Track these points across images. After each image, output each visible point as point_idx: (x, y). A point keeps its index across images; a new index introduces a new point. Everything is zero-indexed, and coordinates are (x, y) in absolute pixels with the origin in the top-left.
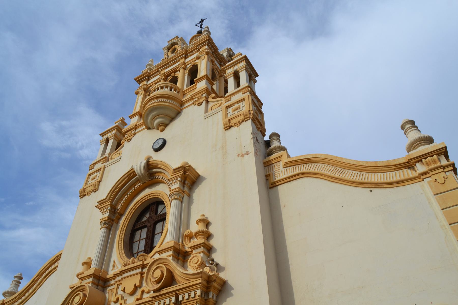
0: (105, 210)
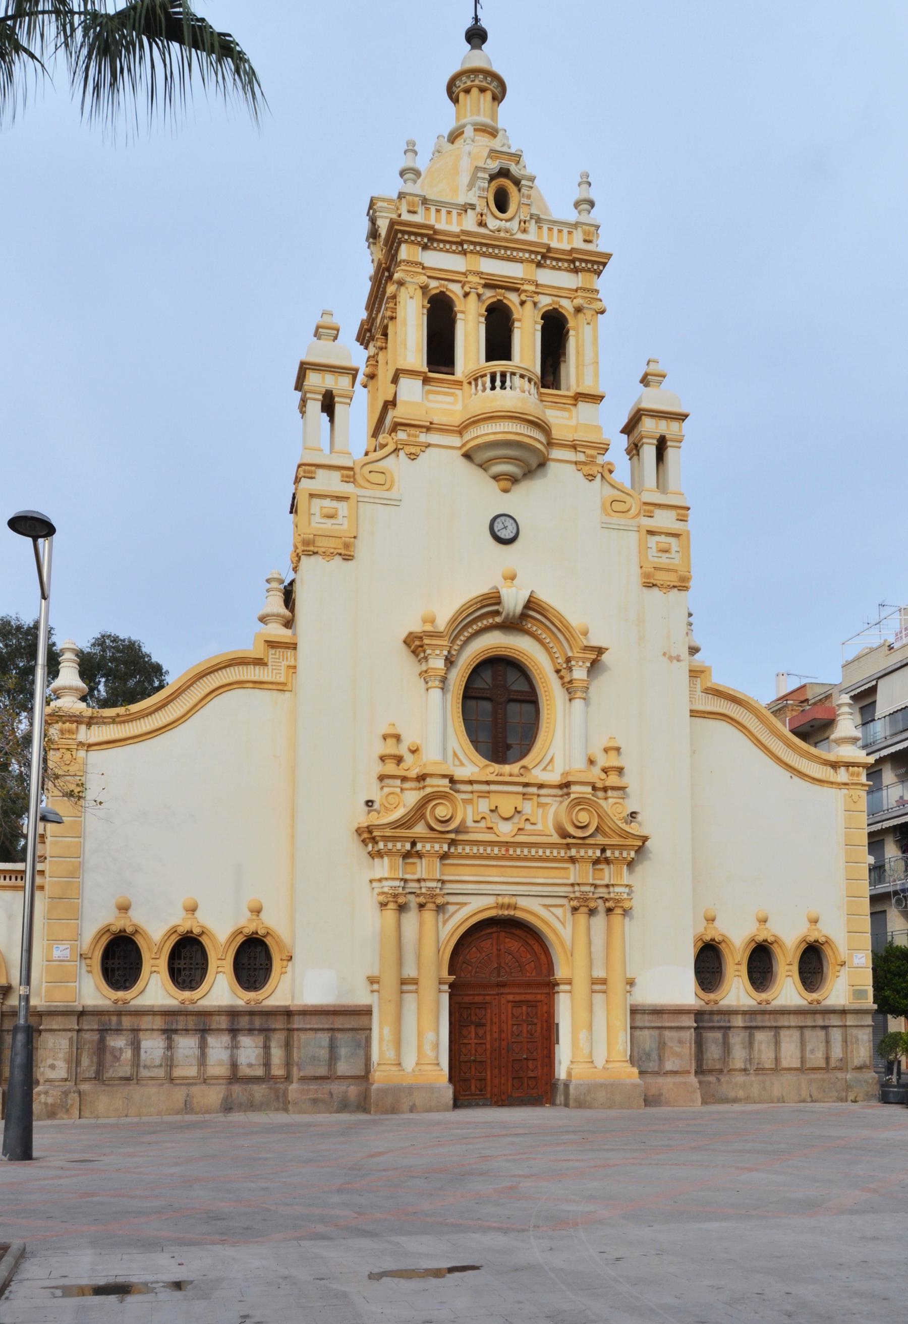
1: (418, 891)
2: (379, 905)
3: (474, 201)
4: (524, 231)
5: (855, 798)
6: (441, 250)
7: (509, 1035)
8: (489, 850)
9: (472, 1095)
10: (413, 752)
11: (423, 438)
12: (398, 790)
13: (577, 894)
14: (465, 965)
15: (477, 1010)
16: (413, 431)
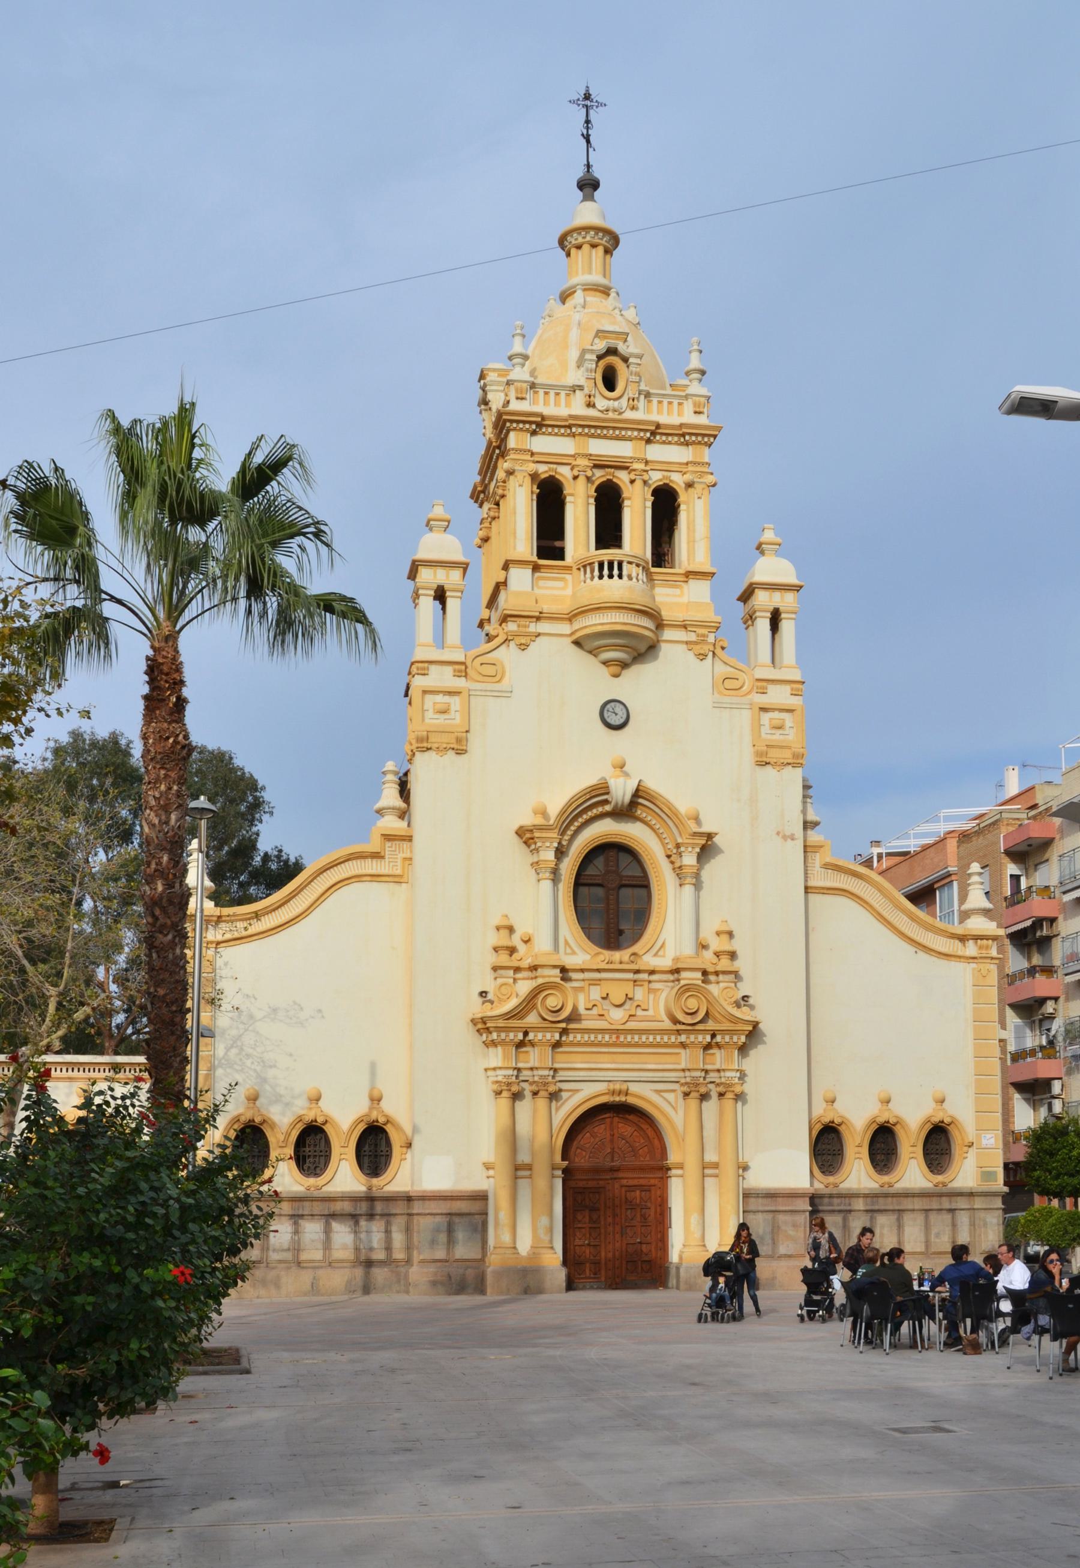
0: (548, 844)
1: (531, 1080)
2: (493, 1094)
3: (582, 382)
4: (633, 408)
5: (984, 972)
6: (550, 434)
7: (623, 1220)
8: (600, 1037)
9: (586, 1278)
10: (526, 942)
11: (533, 627)
12: (511, 981)
13: (688, 1080)
14: (579, 1151)
15: (591, 1195)
16: (522, 621)
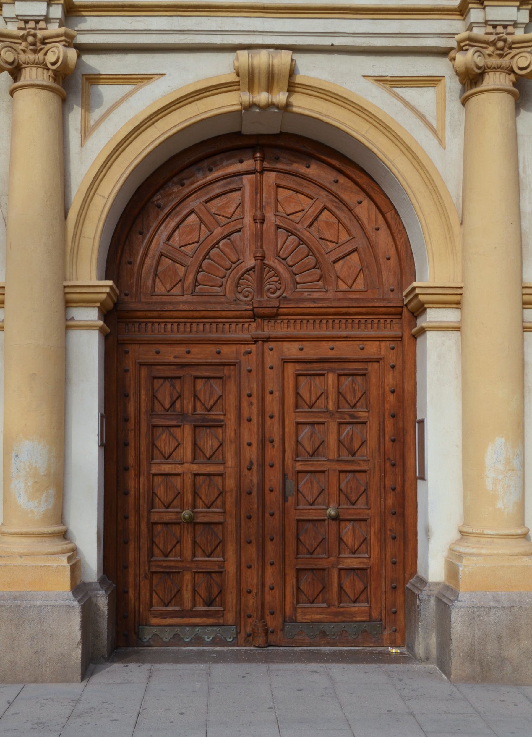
7: (289, 454)
9: (182, 614)
15: (200, 384)
